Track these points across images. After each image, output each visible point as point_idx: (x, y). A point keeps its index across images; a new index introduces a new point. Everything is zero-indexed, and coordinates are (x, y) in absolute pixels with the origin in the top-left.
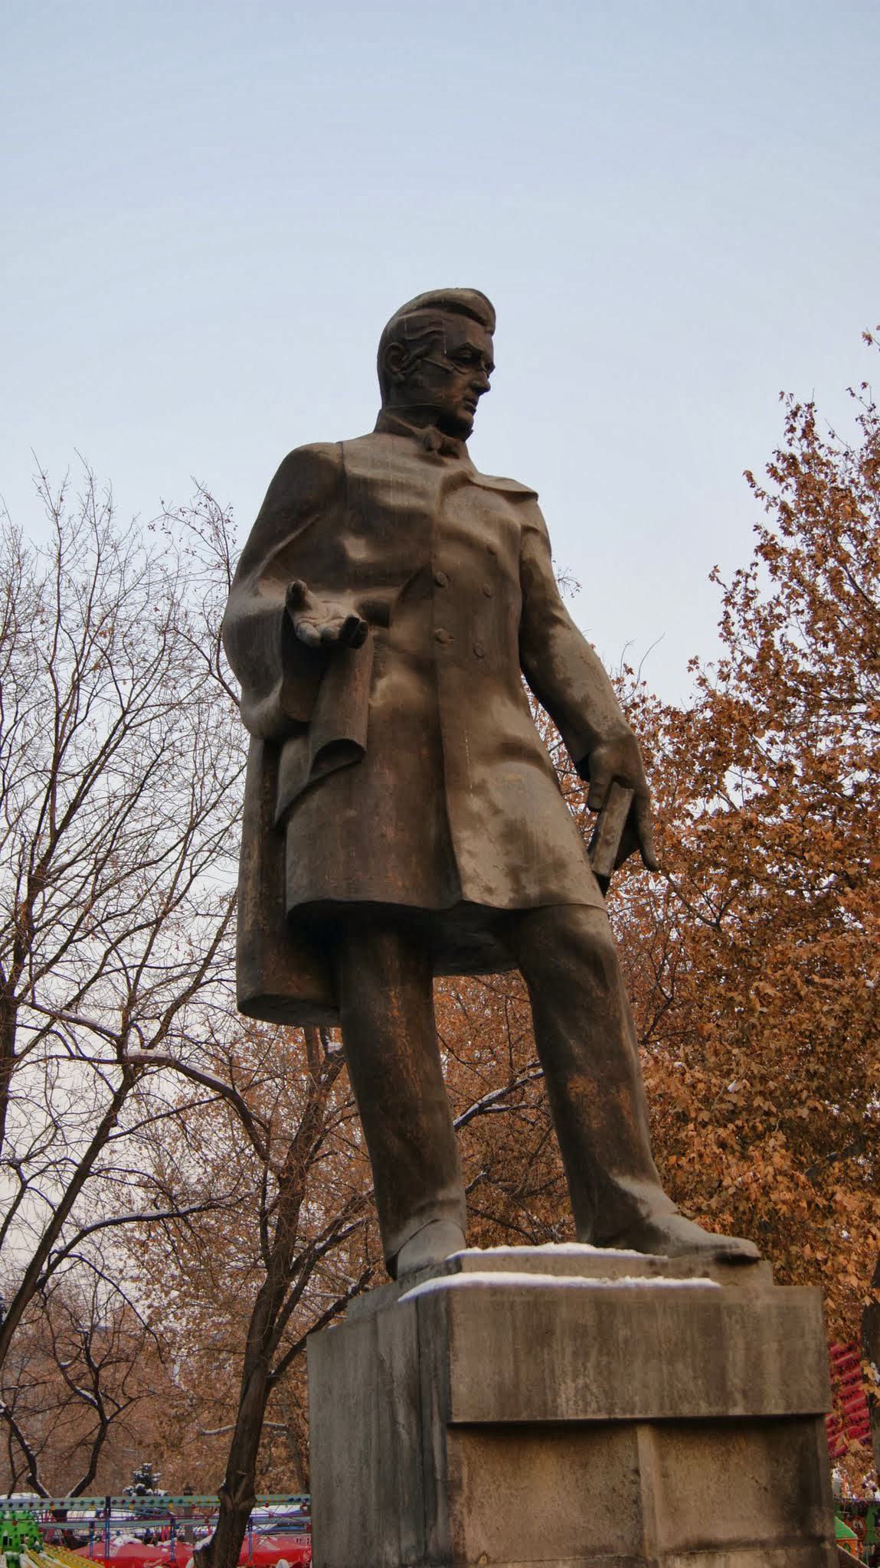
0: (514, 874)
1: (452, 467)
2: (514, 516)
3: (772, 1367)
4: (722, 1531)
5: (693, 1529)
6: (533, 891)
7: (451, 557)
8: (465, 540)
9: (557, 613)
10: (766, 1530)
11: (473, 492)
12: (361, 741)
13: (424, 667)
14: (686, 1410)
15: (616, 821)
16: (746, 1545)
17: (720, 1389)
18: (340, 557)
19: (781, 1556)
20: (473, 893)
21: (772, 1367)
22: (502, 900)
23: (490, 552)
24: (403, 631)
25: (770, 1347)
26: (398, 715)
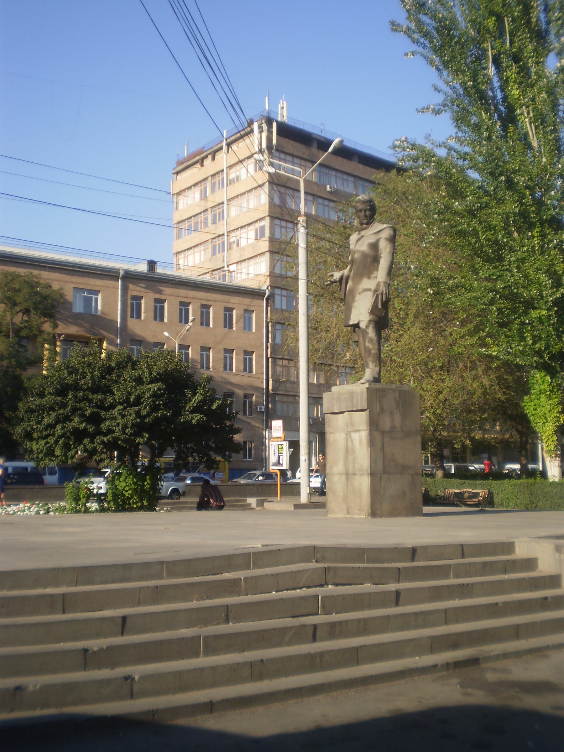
1: (363, 233)
2: (372, 240)
3: (359, 401)
4: (361, 428)
5: (357, 428)
7: (356, 256)
8: (359, 251)
9: (382, 255)
11: (363, 239)
12: (343, 298)
13: (353, 279)
14: (349, 410)
16: (363, 430)
17: (353, 406)
21: (359, 401)
22: (356, 322)
25: (359, 398)
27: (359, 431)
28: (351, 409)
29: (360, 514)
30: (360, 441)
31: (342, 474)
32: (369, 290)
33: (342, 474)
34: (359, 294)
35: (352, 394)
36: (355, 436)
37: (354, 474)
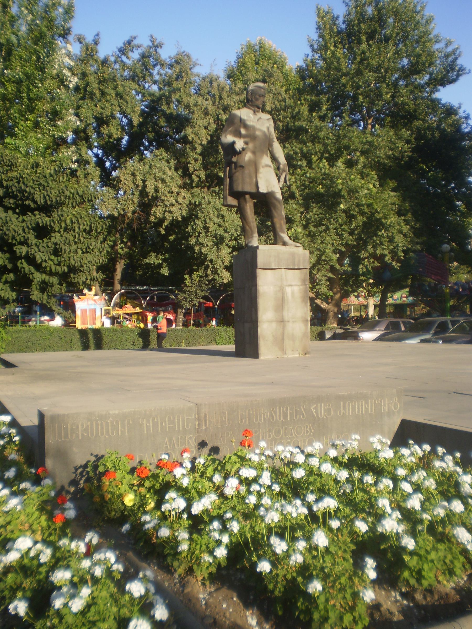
0: (267, 187)
4: (293, 283)
6: (270, 190)
7: (258, 133)
8: (260, 130)
10: (299, 283)
13: (254, 153)
14: (289, 267)
15: (282, 178)
18: (240, 133)
19: (301, 287)
20: (261, 190)
22: (265, 191)
23: (264, 132)
24: (251, 146)
26: (250, 161)
27: (291, 285)
28: (292, 267)
29: (293, 354)
30: (293, 293)
31: (271, 322)
32: (270, 167)
33: (271, 322)
34: (263, 167)
35: (293, 255)
36: (288, 290)
37: (288, 321)
